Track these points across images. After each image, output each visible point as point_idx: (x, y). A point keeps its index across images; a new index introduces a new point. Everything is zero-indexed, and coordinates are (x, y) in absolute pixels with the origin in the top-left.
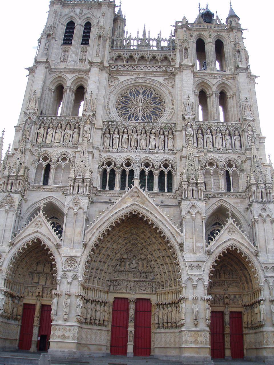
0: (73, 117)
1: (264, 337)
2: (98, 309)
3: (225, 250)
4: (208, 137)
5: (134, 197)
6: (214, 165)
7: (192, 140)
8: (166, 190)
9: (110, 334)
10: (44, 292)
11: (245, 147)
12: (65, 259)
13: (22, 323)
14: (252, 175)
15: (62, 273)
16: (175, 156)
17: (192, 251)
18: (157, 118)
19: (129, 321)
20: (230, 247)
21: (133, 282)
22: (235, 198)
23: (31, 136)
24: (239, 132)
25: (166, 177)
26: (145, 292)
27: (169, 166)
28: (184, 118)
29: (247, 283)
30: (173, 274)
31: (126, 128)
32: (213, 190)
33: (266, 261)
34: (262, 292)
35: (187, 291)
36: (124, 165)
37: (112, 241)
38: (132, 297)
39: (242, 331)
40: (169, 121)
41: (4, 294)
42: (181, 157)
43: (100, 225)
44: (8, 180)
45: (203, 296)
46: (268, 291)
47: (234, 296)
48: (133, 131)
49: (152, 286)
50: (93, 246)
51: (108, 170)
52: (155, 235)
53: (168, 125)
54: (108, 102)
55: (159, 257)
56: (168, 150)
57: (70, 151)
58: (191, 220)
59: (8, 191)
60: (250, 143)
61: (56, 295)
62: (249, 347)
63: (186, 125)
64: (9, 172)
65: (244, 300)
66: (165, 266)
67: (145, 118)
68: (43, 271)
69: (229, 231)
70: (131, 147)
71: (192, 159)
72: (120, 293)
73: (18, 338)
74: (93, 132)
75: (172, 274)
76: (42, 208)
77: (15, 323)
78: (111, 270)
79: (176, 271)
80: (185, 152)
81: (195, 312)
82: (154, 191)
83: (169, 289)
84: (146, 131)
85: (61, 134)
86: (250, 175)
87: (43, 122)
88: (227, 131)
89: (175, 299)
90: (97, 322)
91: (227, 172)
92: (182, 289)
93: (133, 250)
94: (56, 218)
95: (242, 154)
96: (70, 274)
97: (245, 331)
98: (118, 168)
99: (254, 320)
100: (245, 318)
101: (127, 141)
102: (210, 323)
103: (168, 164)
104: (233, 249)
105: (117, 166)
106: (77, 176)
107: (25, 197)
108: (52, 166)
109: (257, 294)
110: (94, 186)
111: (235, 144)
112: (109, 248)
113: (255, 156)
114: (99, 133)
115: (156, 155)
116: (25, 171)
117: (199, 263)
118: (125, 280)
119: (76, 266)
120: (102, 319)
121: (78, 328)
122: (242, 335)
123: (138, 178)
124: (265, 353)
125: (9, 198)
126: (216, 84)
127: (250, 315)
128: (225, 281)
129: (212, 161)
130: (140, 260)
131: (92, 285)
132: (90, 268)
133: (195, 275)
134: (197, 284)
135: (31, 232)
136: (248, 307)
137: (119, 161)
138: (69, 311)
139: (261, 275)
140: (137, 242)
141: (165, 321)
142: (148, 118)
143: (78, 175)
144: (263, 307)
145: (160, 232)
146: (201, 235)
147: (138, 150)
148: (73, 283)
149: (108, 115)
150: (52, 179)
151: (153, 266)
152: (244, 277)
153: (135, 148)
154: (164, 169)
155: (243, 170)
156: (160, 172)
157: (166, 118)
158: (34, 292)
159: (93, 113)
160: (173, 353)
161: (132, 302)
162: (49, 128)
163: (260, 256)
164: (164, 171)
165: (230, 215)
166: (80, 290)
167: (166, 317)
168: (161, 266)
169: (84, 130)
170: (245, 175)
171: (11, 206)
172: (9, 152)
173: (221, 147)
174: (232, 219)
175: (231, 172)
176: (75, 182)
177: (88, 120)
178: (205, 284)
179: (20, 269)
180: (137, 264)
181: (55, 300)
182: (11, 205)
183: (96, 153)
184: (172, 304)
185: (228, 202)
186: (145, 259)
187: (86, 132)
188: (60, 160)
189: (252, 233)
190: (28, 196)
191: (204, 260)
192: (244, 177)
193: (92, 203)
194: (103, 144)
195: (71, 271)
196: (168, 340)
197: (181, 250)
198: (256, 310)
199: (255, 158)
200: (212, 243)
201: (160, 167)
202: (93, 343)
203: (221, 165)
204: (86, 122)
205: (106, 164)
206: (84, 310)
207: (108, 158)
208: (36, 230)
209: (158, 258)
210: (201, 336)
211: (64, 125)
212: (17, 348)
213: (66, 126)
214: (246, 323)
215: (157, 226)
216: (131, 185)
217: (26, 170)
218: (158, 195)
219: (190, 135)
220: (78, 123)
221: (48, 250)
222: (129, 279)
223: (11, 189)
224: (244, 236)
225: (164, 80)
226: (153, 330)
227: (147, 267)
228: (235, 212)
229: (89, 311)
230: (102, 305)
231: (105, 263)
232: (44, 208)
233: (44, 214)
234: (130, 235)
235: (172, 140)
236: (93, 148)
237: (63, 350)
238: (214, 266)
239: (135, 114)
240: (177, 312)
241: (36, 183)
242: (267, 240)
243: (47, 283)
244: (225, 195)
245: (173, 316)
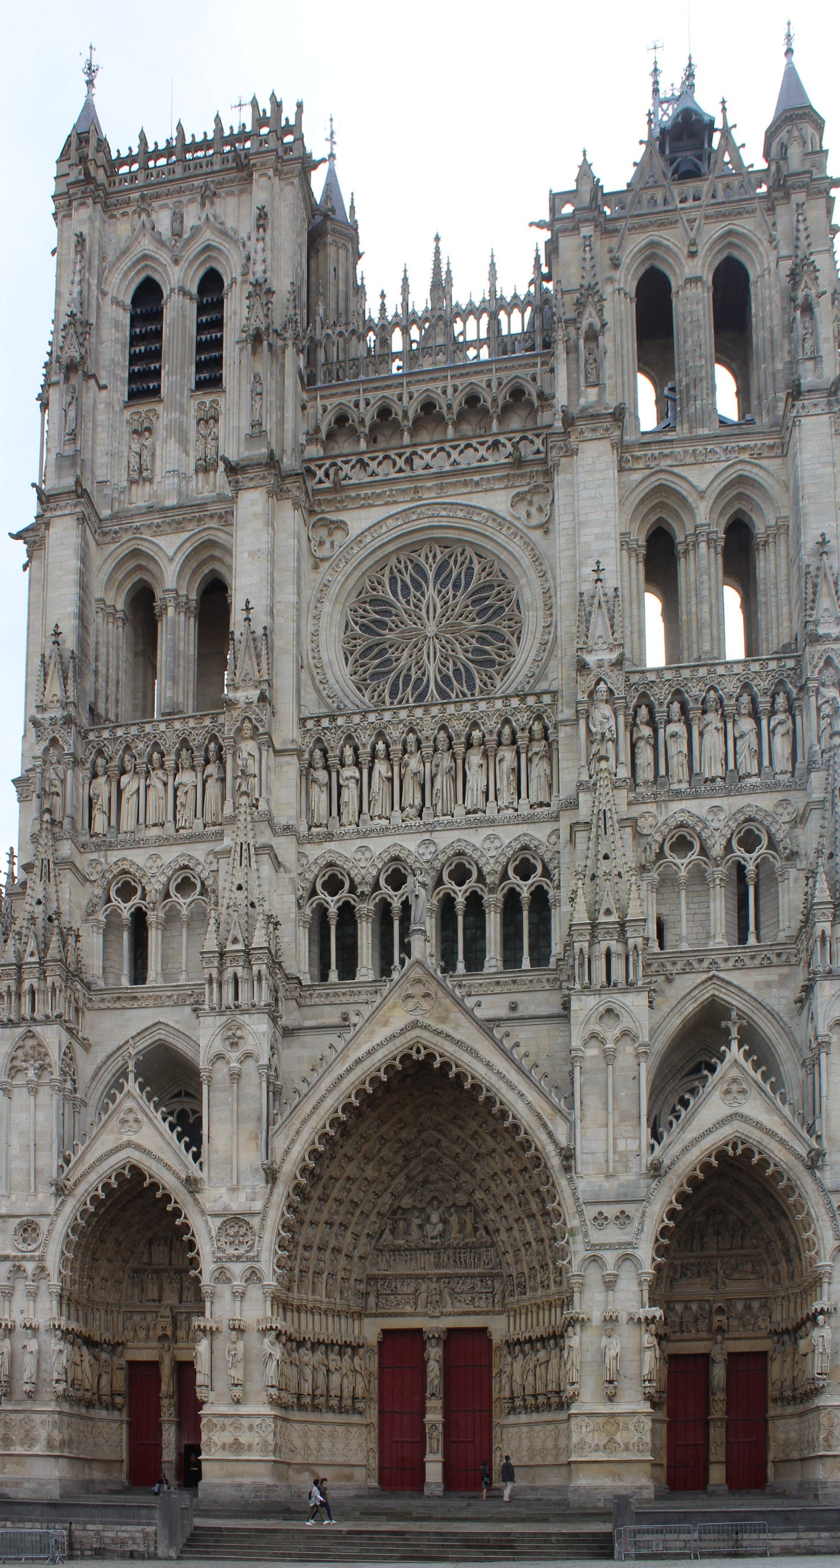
24: (789, 698)
48: (405, 743)
51: (333, 910)
54: (316, 634)
56: (531, 807)
80: (584, 812)
84: (450, 738)
88: (746, 698)
101: (386, 786)
126: (712, 488)
137: (363, 872)
149: (318, 691)
153: (412, 812)
173: (718, 771)
183: (286, 848)
194: (308, 808)
207: (331, 865)
225: (518, 499)
235: (544, 765)
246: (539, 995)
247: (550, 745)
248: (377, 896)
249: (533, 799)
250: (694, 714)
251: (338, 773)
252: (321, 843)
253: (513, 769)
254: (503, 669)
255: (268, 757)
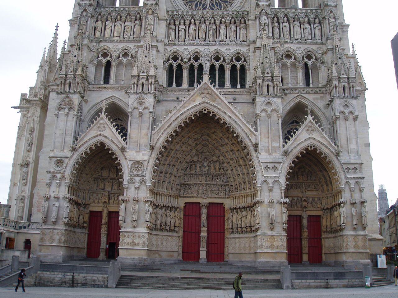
0: (133, 7)
1: (343, 241)
2: (168, 215)
3: (303, 150)
4: (285, 26)
5: (204, 94)
6: (291, 57)
7: (267, 29)
8: (239, 86)
9: (181, 240)
10: (111, 198)
11: (326, 36)
12: (131, 163)
13: (89, 231)
14: (334, 67)
15: (129, 178)
16: (248, 48)
17: (268, 151)
18: (227, 6)
19: (202, 226)
20: (308, 146)
21: (205, 185)
22: (315, 93)
23: (88, 30)
24: (319, 20)
25: (238, 72)
26: (218, 196)
27: (241, 59)
28: (257, 5)
29: (327, 185)
30: (247, 176)
31: (193, 17)
32: (290, 85)
33: (348, 161)
34: (343, 194)
35: (263, 193)
36: (192, 59)
37: (182, 142)
38: (204, 201)
39: (321, 235)
40: (240, 9)
41: (69, 202)
42: (255, 49)
43: (167, 126)
44: (66, 80)
45: (279, 199)
46: (350, 193)
47: (313, 200)
48: (200, 21)
49: (225, 190)
50: (160, 149)
51: (175, 66)
52: (227, 135)
53: (240, 13)
55: (232, 158)
56: (241, 41)
57: (131, 45)
58: (267, 118)
59: (66, 92)
60: (332, 31)
61: (123, 201)
62: (327, 252)
63: (260, 13)
64: (66, 72)
65: (323, 203)
66: (239, 168)
67: (214, 6)
68: (109, 177)
69: (308, 130)
70: (199, 39)
71: (267, 50)
72: (191, 197)
73: (86, 246)
74: (157, 23)
75: (246, 177)
76: (104, 110)
77: (81, 232)
78: (180, 173)
79: (250, 173)
80: (258, 44)
81: (270, 216)
82: (225, 87)
83: (243, 192)
84: (215, 20)
85: (121, 27)
86: (332, 68)
87: (100, 14)
88: (306, 19)
89: (250, 202)
90: (168, 228)
91: (306, 65)
92: (257, 192)
93: (204, 151)
94: (119, 119)
95: (323, 44)
96: (137, 179)
97: (324, 235)
98: (185, 63)
99: (334, 224)
100: (324, 222)
102: (286, 228)
103: (241, 57)
104: (312, 149)
105: (184, 60)
106: (141, 73)
107: (85, 98)
108: (113, 63)
109: (338, 197)
110: (159, 83)
111: (315, 33)
112: (179, 150)
113: (337, 46)
114: (163, 24)
115: (227, 47)
116: (83, 70)
117: (275, 165)
118: (196, 184)
119: (143, 170)
120: (172, 225)
121: (148, 235)
122: (321, 239)
123: (208, 73)
124: (344, 258)
125: (67, 100)
127: (329, 218)
128: (303, 183)
129: (288, 53)
130: (212, 162)
131: (161, 190)
132: (159, 172)
133: (271, 177)
134: (273, 187)
135: (94, 135)
136: (327, 211)
137: (186, 55)
138: (138, 217)
139: (342, 177)
140: (208, 144)
141: (239, 225)
142: (217, 5)
143: (142, 71)
144: (343, 210)
145: (233, 132)
146: (277, 134)
147: (206, 42)
148: (140, 189)
150: (114, 77)
151: (225, 169)
152: (323, 179)
153: (203, 39)
154: (237, 62)
155: (323, 63)
156: (231, 66)
157: (238, 5)
158: (100, 198)
159: (155, 2)
160: (248, 258)
161: (204, 207)
162: (107, 20)
163: (341, 156)
164: (236, 64)
165: (309, 112)
166: (148, 195)
167: (240, 222)
168: (234, 169)
169: (146, 22)
170: (326, 68)
171: (71, 108)
172: (65, 49)
173: (299, 37)
174: (311, 117)
175: (310, 65)
176: (138, 79)
177: (151, 10)
178: (281, 187)
179: (83, 175)
180: (209, 166)
181: (122, 206)
182: (71, 107)
183: (161, 47)
184: (247, 208)
185: (307, 99)
186: (217, 161)
187: (149, 24)
188: (121, 56)
189: (333, 131)
190: (89, 96)
191: (281, 161)
192: (324, 70)
193: (159, 102)
194: (168, 36)
195: (138, 175)
196: (243, 245)
197: (256, 151)
198: (336, 213)
199: (337, 49)
200: (289, 143)
201: (232, 60)
202: (164, 249)
203: (299, 57)
204: (148, 12)
205: (172, 58)
206: (153, 216)
207: (174, 52)
208: (99, 133)
209: (231, 159)
210: (277, 240)
211: (123, 16)
212: (85, 256)
213: (126, 17)
214: (325, 227)
215: (229, 125)
216: (200, 81)
217: (85, 68)
218: (230, 92)
219: (265, 24)
220: (139, 13)
221: (113, 154)
222: (200, 183)
223: (70, 89)
224: (324, 135)
226: (227, 235)
227: (220, 169)
228: (314, 109)
229: (159, 216)
230: (172, 210)
231: (175, 166)
232: (106, 109)
233: (107, 116)
234: (200, 136)
235: (245, 30)
236: (157, 42)
237: (133, 257)
238: (291, 168)
239: (202, 1)
240: (252, 217)
241: (96, 82)
242: (349, 139)
243: (113, 189)
244: (304, 90)
245: (248, 220)
246: (243, 96)
247: (246, 25)
248: (190, 63)
249: (241, 39)
250: (291, 22)
251: (178, 27)
252: (172, 46)
253: (235, 31)
254: (231, 4)
255: (156, 21)
